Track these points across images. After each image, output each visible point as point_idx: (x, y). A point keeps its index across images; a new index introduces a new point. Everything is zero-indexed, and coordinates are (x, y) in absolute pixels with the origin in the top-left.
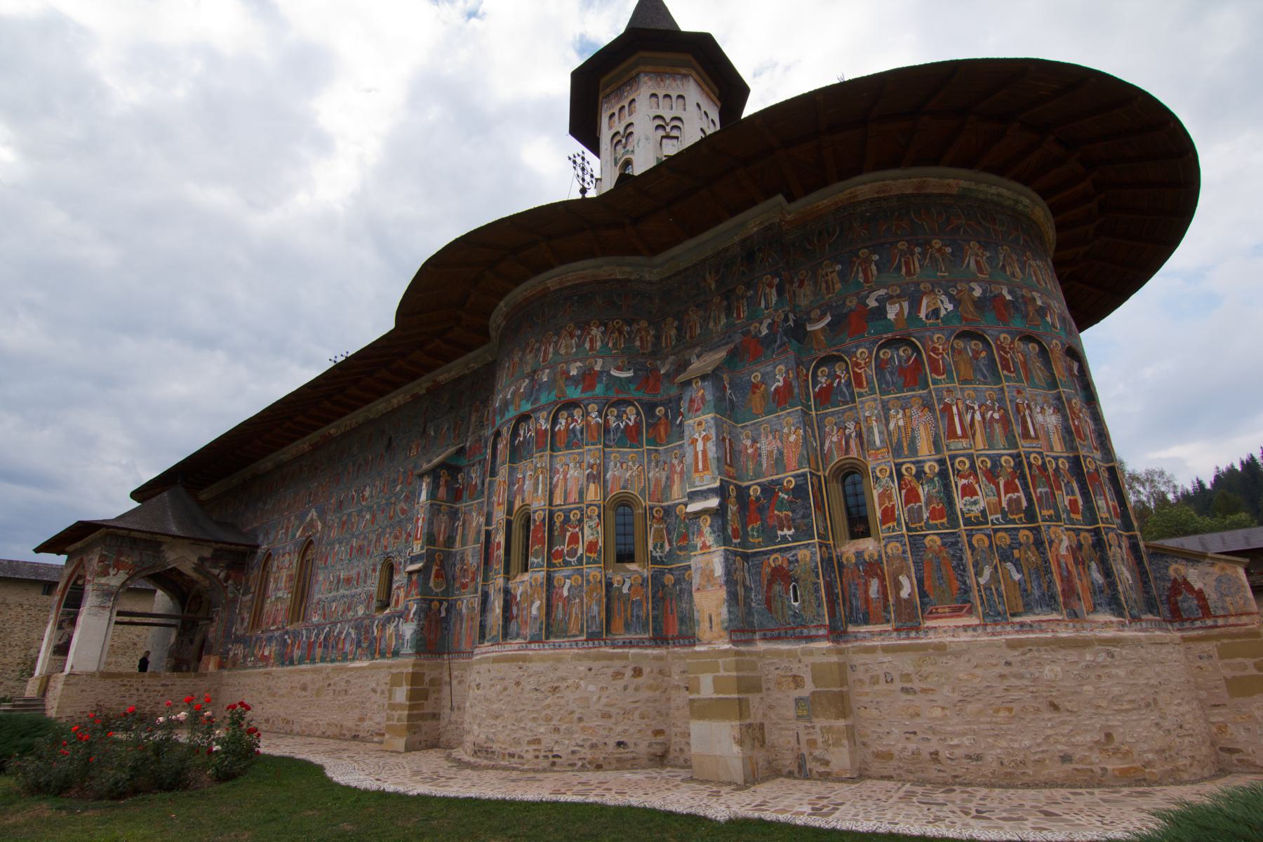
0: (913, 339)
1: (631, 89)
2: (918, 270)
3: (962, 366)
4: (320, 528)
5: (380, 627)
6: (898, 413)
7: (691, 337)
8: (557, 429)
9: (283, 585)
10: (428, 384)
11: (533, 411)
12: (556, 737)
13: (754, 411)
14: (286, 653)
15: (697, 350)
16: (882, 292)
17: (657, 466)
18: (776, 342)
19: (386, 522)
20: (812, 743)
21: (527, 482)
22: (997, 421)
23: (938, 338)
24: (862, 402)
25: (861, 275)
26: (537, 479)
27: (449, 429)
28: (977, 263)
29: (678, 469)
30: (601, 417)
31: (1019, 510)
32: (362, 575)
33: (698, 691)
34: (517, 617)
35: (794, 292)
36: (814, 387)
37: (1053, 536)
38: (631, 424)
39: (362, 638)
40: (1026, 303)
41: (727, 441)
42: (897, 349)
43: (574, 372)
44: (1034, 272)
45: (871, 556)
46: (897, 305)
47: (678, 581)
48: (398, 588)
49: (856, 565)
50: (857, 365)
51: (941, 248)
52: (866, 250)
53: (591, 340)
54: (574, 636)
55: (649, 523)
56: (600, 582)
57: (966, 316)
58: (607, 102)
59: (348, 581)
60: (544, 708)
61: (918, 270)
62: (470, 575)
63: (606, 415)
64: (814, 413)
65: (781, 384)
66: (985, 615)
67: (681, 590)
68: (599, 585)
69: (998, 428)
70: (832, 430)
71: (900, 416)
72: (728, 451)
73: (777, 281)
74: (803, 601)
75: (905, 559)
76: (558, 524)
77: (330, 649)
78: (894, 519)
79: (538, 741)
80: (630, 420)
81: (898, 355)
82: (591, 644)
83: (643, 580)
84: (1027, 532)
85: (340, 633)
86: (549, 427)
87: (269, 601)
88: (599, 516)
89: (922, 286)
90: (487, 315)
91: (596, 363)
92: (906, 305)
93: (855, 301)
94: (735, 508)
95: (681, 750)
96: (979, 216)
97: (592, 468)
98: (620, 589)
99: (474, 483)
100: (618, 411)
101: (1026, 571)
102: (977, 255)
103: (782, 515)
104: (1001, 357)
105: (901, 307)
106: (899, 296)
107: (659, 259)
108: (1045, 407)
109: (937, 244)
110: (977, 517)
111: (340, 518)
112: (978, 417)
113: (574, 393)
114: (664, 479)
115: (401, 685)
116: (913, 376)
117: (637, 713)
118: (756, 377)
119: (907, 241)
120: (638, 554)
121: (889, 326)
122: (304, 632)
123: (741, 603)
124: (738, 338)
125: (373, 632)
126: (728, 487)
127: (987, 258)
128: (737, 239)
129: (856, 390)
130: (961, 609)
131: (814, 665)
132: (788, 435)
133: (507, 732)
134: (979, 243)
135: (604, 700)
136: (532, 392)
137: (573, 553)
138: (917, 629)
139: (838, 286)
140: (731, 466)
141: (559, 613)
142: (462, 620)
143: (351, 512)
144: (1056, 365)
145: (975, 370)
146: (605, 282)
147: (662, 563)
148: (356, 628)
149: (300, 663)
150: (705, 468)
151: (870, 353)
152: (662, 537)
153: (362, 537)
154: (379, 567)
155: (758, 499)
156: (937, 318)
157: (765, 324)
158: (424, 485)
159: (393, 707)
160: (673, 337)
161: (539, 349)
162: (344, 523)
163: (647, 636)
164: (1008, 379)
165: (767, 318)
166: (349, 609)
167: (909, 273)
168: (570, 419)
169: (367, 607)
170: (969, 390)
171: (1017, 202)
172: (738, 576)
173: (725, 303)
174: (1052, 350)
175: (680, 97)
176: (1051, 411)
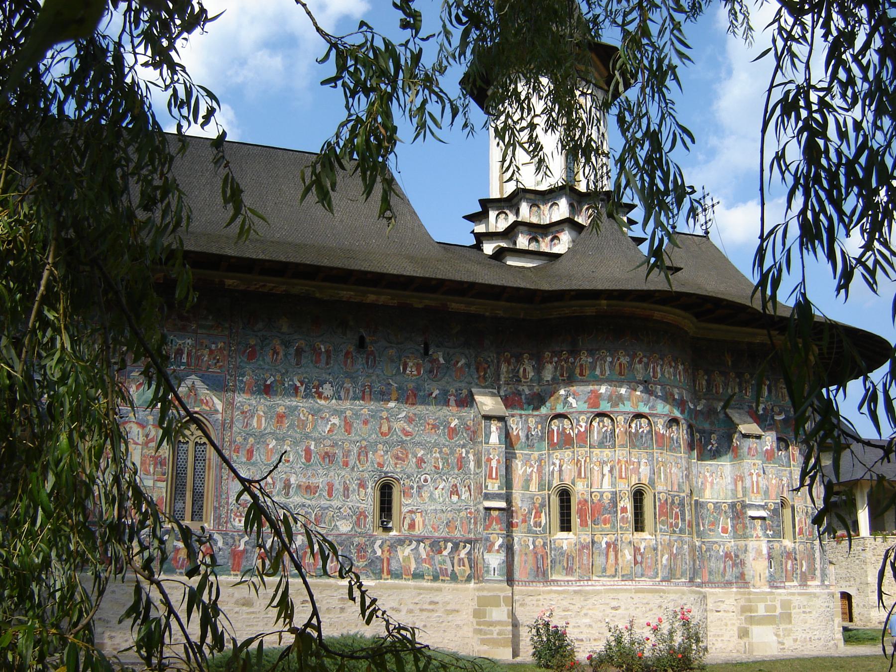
4: (219, 406)
5: (386, 548)
7: (716, 392)
21: (642, 467)
27: (468, 365)
29: (710, 480)
32: (338, 486)
33: (757, 612)
34: (641, 563)
45: (789, 549)
47: (708, 550)
48: (411, 512)
54: (679, 579)
59: (310, 489)
62: (521, 518)
65: (769, 448)
67: (710, 555)
95: (713, 644)
99: (515, 433)
111: (271, 408)
114: (700, 483)
115: (499, 605)
128: (746, 340)
131: (781, 600)
132: (772, 479)
137: (677, 525)
138: (806, 585)
143: (297, 407)
150: (758, 492)
154: (370, 484)
158: (493, 428)
159: (491, 624)
160: (704, 387)
161: (647, 366)
162: (281, 417)
165: (762, 403)
169: (357, 523)
173: (738, 380)
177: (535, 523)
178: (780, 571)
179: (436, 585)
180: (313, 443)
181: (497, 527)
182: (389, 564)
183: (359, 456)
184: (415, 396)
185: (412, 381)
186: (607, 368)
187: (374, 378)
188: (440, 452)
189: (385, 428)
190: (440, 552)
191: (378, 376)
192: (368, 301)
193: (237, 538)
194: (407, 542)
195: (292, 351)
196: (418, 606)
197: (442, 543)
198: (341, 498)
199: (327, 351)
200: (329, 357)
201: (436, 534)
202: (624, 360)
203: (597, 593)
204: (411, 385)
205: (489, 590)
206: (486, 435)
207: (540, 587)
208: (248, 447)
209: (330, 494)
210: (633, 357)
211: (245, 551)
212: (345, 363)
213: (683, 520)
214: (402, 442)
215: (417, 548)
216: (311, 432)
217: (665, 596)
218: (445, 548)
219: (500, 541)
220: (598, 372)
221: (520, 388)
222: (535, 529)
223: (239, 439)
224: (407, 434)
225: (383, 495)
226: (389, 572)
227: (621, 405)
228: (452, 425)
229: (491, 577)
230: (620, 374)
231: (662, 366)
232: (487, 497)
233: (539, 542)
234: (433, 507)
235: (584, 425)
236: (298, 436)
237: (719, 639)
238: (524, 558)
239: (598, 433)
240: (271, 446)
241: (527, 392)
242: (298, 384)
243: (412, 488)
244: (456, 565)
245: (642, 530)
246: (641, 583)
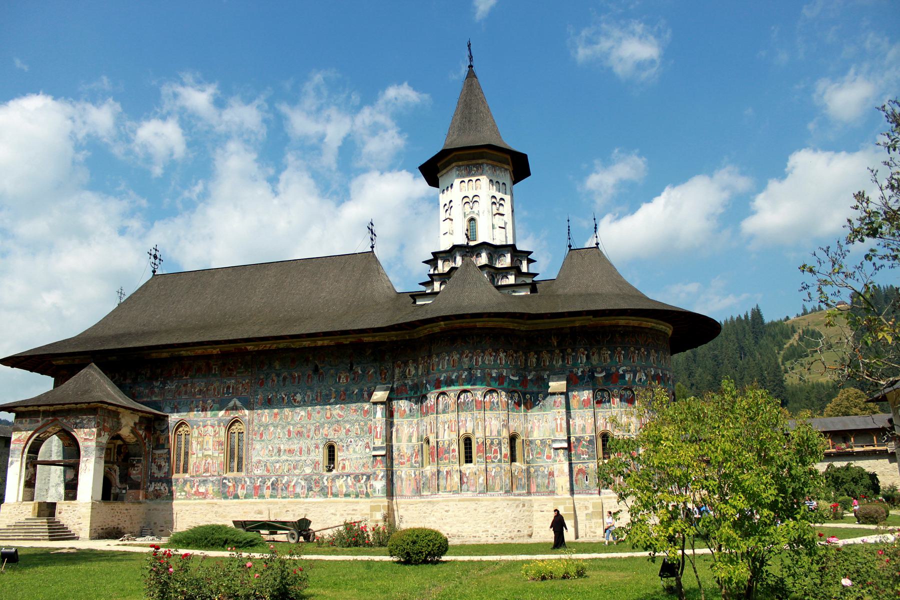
5: (330, 481)
7: (544, 365)
9: (211, 447)
10: (353, 340)
12: (495, 529)
14: (228, 491)
15: (548, 372)
16: (625, 368)
19: (323, 420)
20: (591, 527)
26: (478, 423)
27: (375, 372)
29: (537, 425)
32: (305, 449)
34: (467, 483)
39: (313, 486)
43: (494, 375)
48: (343, 460)
53: (500, 359)
58: (458, 170)
59: (290, 451)
60: (489, 519)
62: (406, 459)
65: (586, 398)
73: (586, 352)
76: (488, 445)
77: (280, 491)
79: (488, 531)
85: (289, 482)
87: (195, 456)
92: (632, 375)
95: (538, 533)
98: (514, 473)
99: (403, 409)
103: (584, 450)
106: (630, 371)
114: (529, 428)
117: (524, 520)
119: (634, 348)
121: (626, 383)
122: (247, 479)
125: (324, 483)
128: (568, 326)
129: (612, 405)
133: (471, 528)
135: (513, 516)
137: (495, 458)
141: (490, 482)
142: (402, 481)
146: (505, 329)
147: (529, 463)
148: (306, 480)
149: (245, 498)
150: (561, 431)
153: (299, 426)
154: (321, 446)
155: (574, 442)
161: (472, 358)
163: (524, 492)
166: (295, 468)
169: (315, 468)
173: (562, 354)
175: (504, 184)
177: (415, 461)
179: (357, 500)
180: (292, 427)
181: (380, 466)
182: (331, 489)
183: (315, 431)
184: (345, 394)
185: (343, 386)
186: (446, 363)
187: (322, 387)
188: (359, 425)
189: (328, 415)
190: (359, 481)
191: (325, 386)
192: (319, 345)
193: (256, 479)
194: (341, 477)
195: (281, 378)
196: (346, 512)
197: (360, 477)
198: (306, 455)
199: (299, 376)
200: (299, 380)
201: (357, 472)
202: (456, 357)
203: (438, 502)
204: (342, 389)
205: (374, 502)
206: (374, 413)
207: (417, 499)
208: (261, 431)
209: (301, 454)
210: (461, 355)
211: (260, 486)
212: (308, 381)
213: (501, 454)
214: (338, 421)
215: (346, 480)
216: (291, 421)
217: (479, 503)
218: (362, 479)
219: (382, 474)
220: (440, 367)
221: (406, 382)
222: (415, 465)
223: (256, 429)
224: (340, 416)
225: (330, 451)
226: (332, 494)
228: (366, 409)
229: (377, 494)
230: (453, 366)
231: (483, 357)
232: (375, 449)
233: (417, 473)
234: (355, 457)
235: (433, 400)
236: (284, 423)
237: (543, 530)
238: (408, 482)
239: (442, 404)
240: (271, 431)
241: (410, 383)
242: (284, 396)
243: (343, 446)
244: (368, 488)
245: (471, 462)
246: (465, 495)
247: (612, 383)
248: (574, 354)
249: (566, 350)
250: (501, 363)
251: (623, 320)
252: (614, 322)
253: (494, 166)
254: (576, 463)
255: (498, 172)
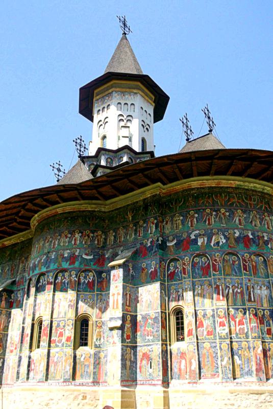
0: (207, 255)
1: (108, 99)
2: (213, 223)
3: (227, 268)
6: (199, 287)
7: (120, 242)
8: (57, 282)
11: (47, 272)
13: (142, 281)
15: (122, 248)
16: (197, 232)
17: (100, 302)
18: (153, 250)
22: (239, 293)
23: (218, 255)
24: (185, 281)
25: (190, 223)
26: (46, 305)
27: (8, 270)
28: (240, 220)
30: (77, 278)
31: (243, 333)
34: (34, 370)
35: (163, 226)
36: (168, 271)
37: (255, 345)
38: (90, 281)
40: (259, 239)
41: (128, 295)
42: (202, 258)
44: (267, 223)
46: (202, 239)
49: (177, 354)
50: (184, 264)
51: (224, 213)
52: (193, 212)
53: (75, 240)
54: (58, 380)
55: (95, 328)
56: (71, 355)
57: (230, 245)
61: (213, 223)
62: (15, 346)
63: (79, 276)
64: (166, 283)
65: (153, 270)
66: (223, 378)
68: (70, 357)
69: (239, 295)
70: (173, 292)
71: (199, 288)
72: (128, 299)
74: (154, 369)
75: (194, 352)
78: (192, 335)
80: (90, 279)
81: (202, 261)
82: (65, 383)
83: (91, 355)
84: (246, 343)
86: (53, 281)
88: (72, 325)
89: (214, 231)
90: (30, 219)
91: (76, 251)
92: (206, 239)
93: (186, 235)
94: (129, 326)
96: (244, 197)
97: (71, 302)
98: (80, 359)
99: (19, 299)
100: (85, 275)
101: (243, 360)
102: (240, 216)
103: (149, 330)
104: (244, 265)
105: (204, 239)
106: (203, 235)
107: (108, 202)
108: (262, 287)
109: (223, 211)
110: (224, 336)
112: (231, 291)
113: (65, 265)
116: (206, 271)
118: (144, 265)
120: (89, 342)
123: (128, 368)
124: (138, 246)
126: (126, 316)
127: (245, 218)
128: (141, 198)
129: (183, 275)
130: (215, 375)
134: (242, 210)
136: (47, 263)
137: (60, 341)
139: (181, 226)
140: (129, 306)
144: (270, 268)
145: (232, 270)
146: (84, 211)
147: (100, 347)
151: (190, 259)
152: (100, 336)
155: (140, 321)
156: (218, 246)
157: (149, 241)
160: (112, 240)
161: (51, 242)
163: (89, 381)
164: (245, 274)
165: (150, 238)
167: (209, 224)
168: (63, 277)
170: (228, 279)
171: (263, 189)
172: (128, 356)
173: (135, 228)
174: (269, 261)
175: (132, 104)
176: (265, 288)
178: (158, 370)
227: (35, 271)
247: (183, 250)
248: (145, 225)
249: (138, 222)
250: (75, 243)
251: (194, 181)
252: (186, 186)
253: (122, 92)
254: (141, 346)
255: (127, 96)
